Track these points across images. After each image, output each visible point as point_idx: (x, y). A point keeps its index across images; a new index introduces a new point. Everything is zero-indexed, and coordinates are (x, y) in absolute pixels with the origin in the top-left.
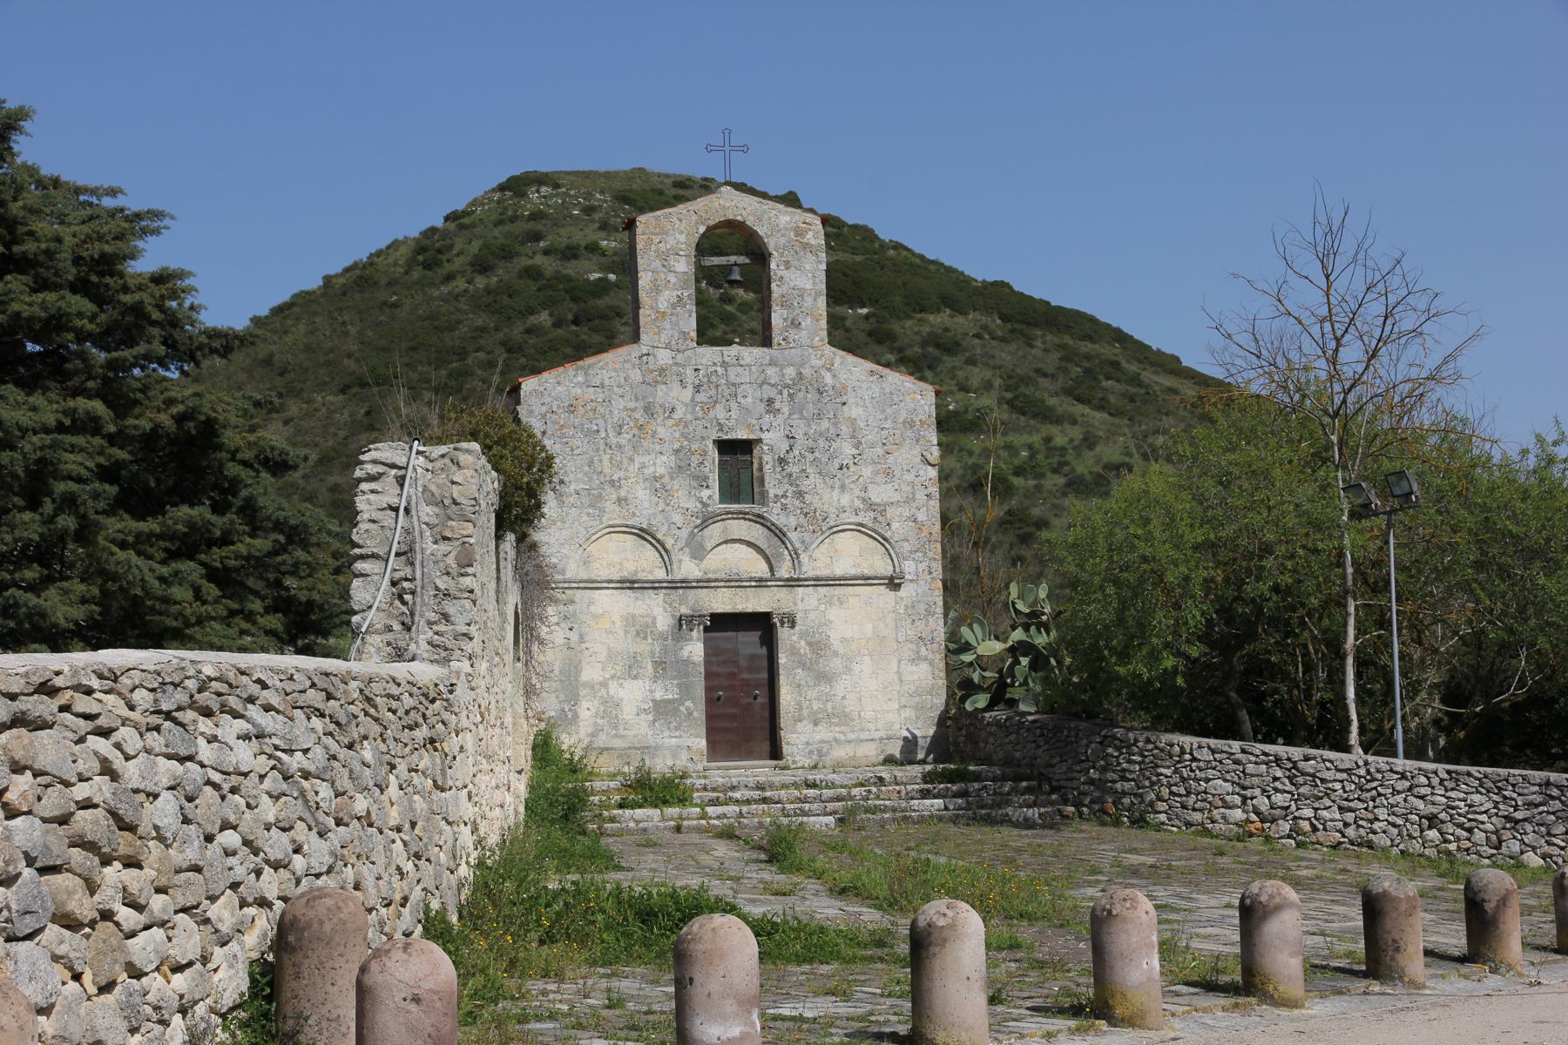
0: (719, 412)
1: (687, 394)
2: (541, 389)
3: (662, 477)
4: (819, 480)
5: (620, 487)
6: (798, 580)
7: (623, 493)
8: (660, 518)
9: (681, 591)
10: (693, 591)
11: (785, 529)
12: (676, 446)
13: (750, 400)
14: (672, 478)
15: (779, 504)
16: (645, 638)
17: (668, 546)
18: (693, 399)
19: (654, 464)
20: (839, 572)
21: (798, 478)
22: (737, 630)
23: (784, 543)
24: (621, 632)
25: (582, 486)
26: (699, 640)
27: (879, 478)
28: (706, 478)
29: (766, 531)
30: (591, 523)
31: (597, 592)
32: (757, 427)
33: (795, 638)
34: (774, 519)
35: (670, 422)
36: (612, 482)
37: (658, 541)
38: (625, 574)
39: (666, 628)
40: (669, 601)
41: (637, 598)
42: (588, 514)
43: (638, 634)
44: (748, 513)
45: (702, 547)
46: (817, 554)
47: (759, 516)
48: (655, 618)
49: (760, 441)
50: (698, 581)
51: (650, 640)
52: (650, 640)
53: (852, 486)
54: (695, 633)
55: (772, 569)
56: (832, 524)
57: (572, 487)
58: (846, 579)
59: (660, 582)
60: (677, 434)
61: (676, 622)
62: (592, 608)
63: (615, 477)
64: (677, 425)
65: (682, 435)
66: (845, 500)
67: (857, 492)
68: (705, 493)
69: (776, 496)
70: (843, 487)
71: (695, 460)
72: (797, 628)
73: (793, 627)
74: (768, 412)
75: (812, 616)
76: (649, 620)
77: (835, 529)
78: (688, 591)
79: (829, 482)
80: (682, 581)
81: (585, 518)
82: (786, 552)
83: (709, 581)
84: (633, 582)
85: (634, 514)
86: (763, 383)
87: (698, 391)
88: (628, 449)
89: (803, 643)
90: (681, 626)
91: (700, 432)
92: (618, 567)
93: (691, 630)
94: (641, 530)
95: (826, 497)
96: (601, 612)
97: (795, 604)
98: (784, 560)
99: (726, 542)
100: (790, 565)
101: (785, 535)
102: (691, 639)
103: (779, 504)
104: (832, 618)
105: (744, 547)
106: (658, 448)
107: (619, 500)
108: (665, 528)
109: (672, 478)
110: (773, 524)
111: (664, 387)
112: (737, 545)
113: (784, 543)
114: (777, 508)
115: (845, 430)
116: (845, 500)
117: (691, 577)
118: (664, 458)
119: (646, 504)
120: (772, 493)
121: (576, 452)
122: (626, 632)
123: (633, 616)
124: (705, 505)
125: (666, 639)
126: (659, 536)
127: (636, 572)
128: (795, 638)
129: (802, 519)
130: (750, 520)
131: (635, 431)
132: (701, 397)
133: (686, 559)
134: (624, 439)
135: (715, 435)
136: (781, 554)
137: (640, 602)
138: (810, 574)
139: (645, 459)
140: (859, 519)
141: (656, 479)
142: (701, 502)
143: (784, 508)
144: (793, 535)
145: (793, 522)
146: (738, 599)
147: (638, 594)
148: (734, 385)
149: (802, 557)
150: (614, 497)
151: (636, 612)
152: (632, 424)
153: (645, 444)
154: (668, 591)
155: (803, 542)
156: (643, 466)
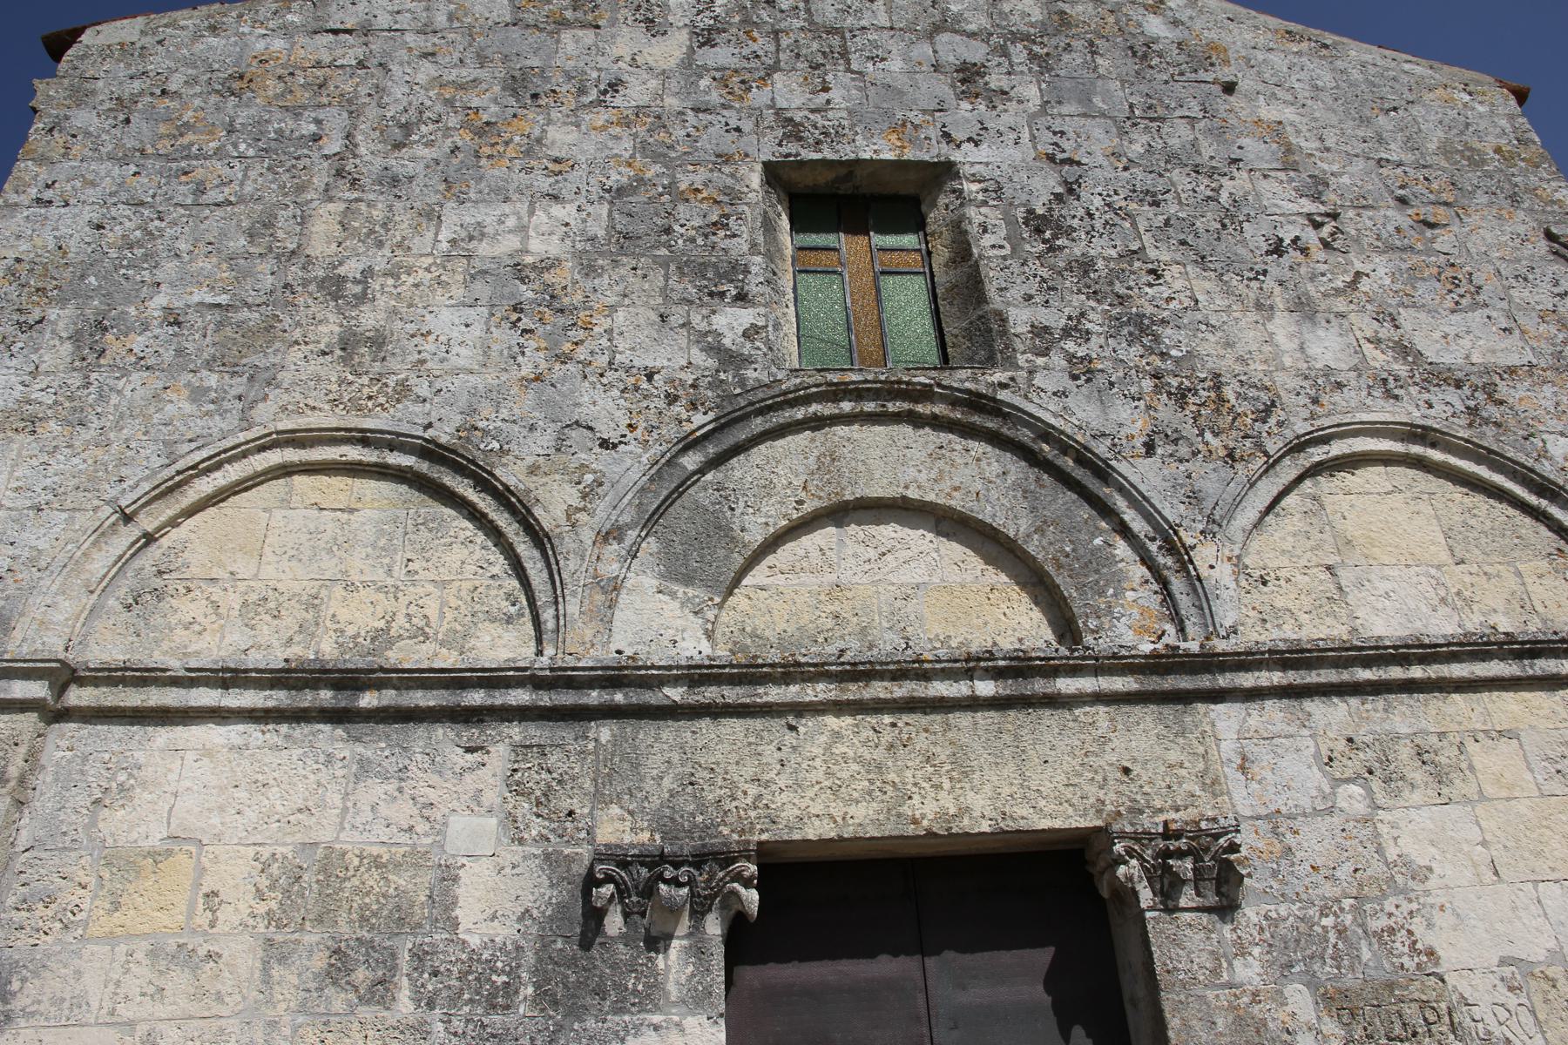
0: (789, 92)
1: (670, 50)
2: (148, 41)
3: (548, 265)
4: (1204, 285)
5: (362, 298)
6: (1209, 662)
7: (368, 319)
8: (524, 404)
9: (605, 732)
10: (669, 732)
11: (1102, 448)
12: (616, 178)
13: (896, 65)
14: (590, 270)
15: (1057, 360)
16: (379, 994)
17: (549, 516)
18: (688, 62)
19: (522, 229)
20: (1384, 626)
21: (1115, 275)
22: (923, 948)
23: (1105, 510)
24: (242, 955)
25: (202, 295)
26: (696, 1000)
27: (1425, 291)
28: (736, 270)
29: (1016, 468)
30: (198, 425)
31: (163, 736)
32: (934, 133)
33: (1249, 971)
34: (1046, 411)
35: (601, 117)
36: (333, 287)
37: (503, 496)
38: (327, 649)
39: (505, 932)
40: (535, 779)
41: (364, 768)
42: (198, 394)
43: (339, 966)
44: (925, 394)
45: (722, 531)
46: (1265, 552)
47: (978, 402)
48: (449, 876)
49: (944, 171)
50: (697, 675)
51: (405, 1004)
52: (405, 1004)
53: (1340, 305)
54: (674, 963)
55: (1066, 627)
56: (1301, 427)
57: (161, 300)
58: (1429, 653)
59: (492, 680)
60: (625, 147)
61: (566, 894)
62: (114, 823)
63: (352, 268)
64: (625, 123)
65: (644, 147)
66: (1327, 347)
67: (1365, 325)
68: (731, 322)
69: (1039, 331)
70: (1304, 308)
71: (690, 217)
72: (1250, 913)
73: (1226, 909)
74: (964, 96)
75: (1314, 842)
76: (415, 886)
77: (1317, 454)
78: (646, 732)
79: (1251, 292)
80: (613, 678)
81: (179, 405)
82: (1122, 549)
83: (751, 674)
84: (350, 680)
85: (403, 390)
86: (937, 29)
87: (709, 42)
88: (425, 192)
89: (1300, 1000)
90: (594, 917)
91: (714, 138)
92: (289, 622)
93: (656, 942)
94: (432, 452)
95: (1248, 335)
96: (155, 835)
97: (1213, 785)
98: (1118, 580)
99: (841, 513)
100: (1154, 602)
101: (1103, 472)
102: (651, 997)
103: (1057, 360)
104: (1421, 855)
105: (920, 539)
106: (544, 183)
107: (347, 344)
108: (544, 440)
109: (590, 270)
110: (1046, 433)
111: (588, 36)
112: (889, 532)
113: (1105, 510)
114: (1052, 374)
115: (1254, 149)
116: (1327, 347)
117: (659, 656)
118: (558, 211)
119: (464, 356)
120: (1020, 319)
121: (213, 195)
122: (275, 953)
123: (331, 864)
124: (730, 359)
125: (507, 994)
126: (510, 474)
127: (382, 637)
128: (1249, 971)
129: (1166, 411)
130: (937, 423)
131: (464, 139)
132: (722, 55)
133: (643, 582)
134: (417, 158)
135: (768, 149)
136: (1101, 560)
137: (375, 790)
138: (1253, 636)
139: (487, 215)
140: (1408, 411)
141: (519, 272)
142: (716, 349)
143: (1082, 370)
144: (1145, 474)
145: (1130, 420)
146: (907, 769)
147: (377, 746)
148: (832, 31)
149: (1204, 555)
150: (329, 330)
151: (350, 841)
152: (453, 121)
153: (494, 173)
154: (536, 732)
155: (1194, 498)
156: (477, 233)
